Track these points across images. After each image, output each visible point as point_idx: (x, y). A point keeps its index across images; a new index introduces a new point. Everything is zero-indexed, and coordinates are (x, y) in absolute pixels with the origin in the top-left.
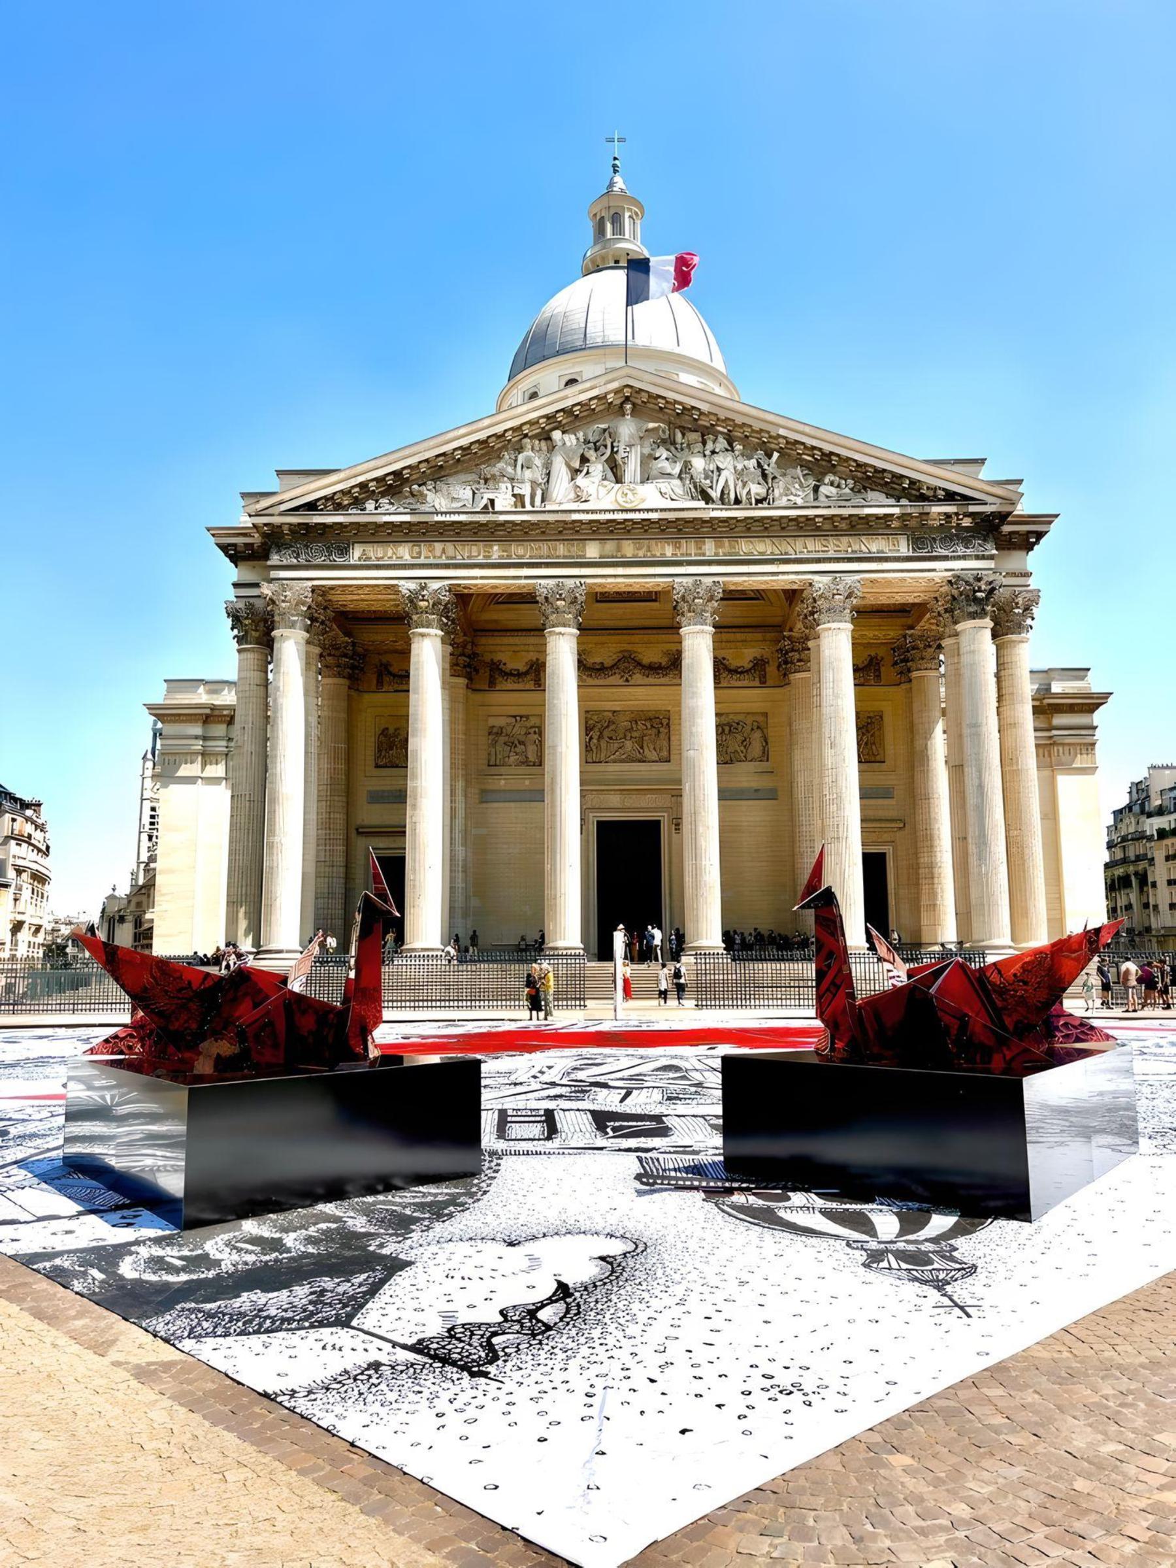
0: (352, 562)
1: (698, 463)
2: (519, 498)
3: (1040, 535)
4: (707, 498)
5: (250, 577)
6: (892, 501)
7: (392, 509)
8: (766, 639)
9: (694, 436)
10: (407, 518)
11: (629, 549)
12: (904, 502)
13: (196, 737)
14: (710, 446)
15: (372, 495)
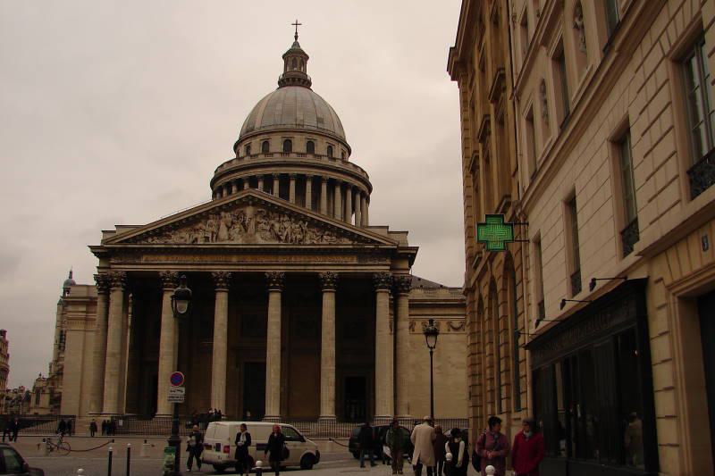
0: (142, 262)
1: (277, 225)
2: (207, 238)
3: (414, 255)
4: (280, 240)
5: (103, 265)
6: (350, 242)
7: (158, 242)
8: (303, 293)
9: (275, 214)
10: (163, 246)
11: (249, 259)
12: (356, 242)
13: (83, 312)
14: (281, 219)
15: (152, 237)
